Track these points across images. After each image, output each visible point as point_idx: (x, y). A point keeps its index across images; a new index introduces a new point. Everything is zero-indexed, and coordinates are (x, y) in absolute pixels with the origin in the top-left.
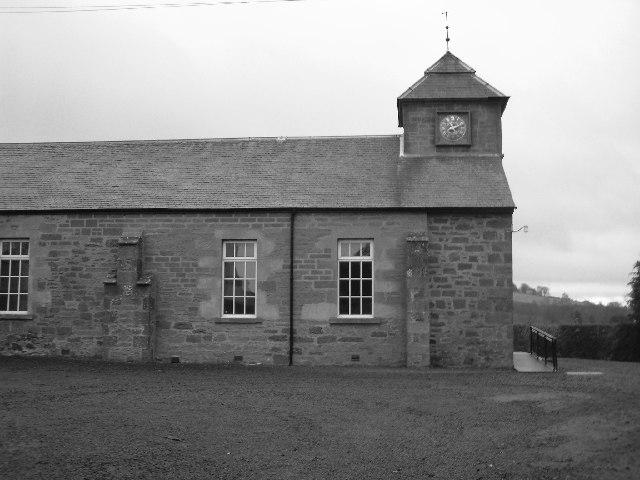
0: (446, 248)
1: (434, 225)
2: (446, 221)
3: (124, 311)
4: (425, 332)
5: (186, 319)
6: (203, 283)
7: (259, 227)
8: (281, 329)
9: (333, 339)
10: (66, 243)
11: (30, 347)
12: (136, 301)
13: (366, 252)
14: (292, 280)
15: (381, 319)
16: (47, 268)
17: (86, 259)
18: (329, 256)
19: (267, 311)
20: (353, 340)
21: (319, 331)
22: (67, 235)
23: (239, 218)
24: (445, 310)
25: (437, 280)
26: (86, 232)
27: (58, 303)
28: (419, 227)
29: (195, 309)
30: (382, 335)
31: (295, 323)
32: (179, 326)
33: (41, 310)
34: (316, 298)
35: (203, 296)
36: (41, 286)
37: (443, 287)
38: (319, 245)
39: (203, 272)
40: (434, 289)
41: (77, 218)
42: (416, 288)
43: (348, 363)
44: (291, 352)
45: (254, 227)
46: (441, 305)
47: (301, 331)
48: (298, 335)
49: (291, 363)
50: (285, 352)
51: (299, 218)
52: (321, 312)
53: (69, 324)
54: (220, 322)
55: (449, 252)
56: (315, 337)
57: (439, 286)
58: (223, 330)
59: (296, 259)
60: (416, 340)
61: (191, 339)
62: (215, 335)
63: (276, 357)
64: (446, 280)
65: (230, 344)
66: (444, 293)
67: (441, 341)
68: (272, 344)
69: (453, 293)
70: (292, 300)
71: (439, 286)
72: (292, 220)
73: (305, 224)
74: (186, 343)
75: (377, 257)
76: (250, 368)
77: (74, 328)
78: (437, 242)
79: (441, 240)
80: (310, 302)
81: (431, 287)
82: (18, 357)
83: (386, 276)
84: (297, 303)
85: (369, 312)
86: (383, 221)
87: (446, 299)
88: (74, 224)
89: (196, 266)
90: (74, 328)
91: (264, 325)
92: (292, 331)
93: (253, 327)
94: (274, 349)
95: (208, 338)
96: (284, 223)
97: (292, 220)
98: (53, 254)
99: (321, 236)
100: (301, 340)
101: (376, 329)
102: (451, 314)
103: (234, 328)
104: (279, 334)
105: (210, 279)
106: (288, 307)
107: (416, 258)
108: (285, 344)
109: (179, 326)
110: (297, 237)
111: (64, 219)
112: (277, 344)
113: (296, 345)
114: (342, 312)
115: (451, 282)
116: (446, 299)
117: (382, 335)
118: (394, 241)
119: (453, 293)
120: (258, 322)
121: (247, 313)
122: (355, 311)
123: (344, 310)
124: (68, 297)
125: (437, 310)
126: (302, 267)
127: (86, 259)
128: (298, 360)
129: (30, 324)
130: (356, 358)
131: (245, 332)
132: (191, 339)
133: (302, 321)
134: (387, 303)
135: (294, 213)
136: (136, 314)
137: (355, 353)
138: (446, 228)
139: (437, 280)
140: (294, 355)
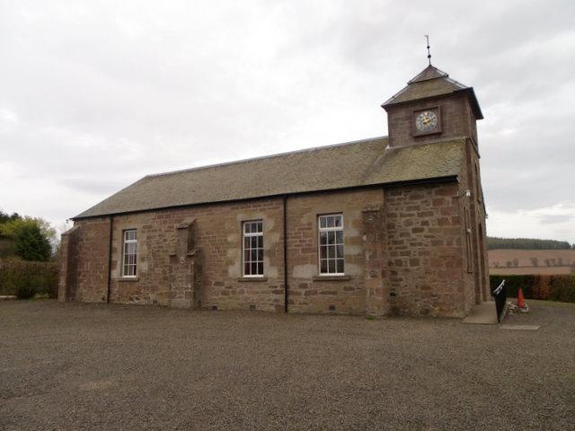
0: (402, 215)
1: (390, 197)
2: (400, 194)
3: (180, 275)
4: (380, 286)
5: (221, 280)
6: (231, 253)
7: (264, 210)
8: (279, 285)
9: (315, 293)
10: (156, 230)
11: (137, 299)
12: (187, 267)
13: (337, 224)
14: (285, 248)
15: (349, 276)
16: (145, 247)
17: (165, 240)
18: (310, 229)
19: (272, 272)
20: (330, 293)
21: (305, 286)
22: (156, 225)
23: (275, 203)
24: (403, 267)
25: (395, 242)
26: (165, 222)
27: (151, 269)
28: (377, 200)
29: (226, 272)
30: (352, 289)
31: (289, 280)
32: (217, 284)
33: (142, 274)
34: (303, 261)
35: (231, 263)
36: (143, 260)
37: (399, 248)
38: (304, 220)
39: (230, 245)
40: (393, 250)
41: (160, 214)
42: (370, 250)
43: (325, 312)
44: (286, 303)
45: (261, 210)
46: (399, 263)
47: (293, 287)
48: (292, 289)
49: (286, 311)
50: (282, 303)
51: (115, 219)
52: (305, 272)
53: (156, 283)
54: (241, 281)
55: (404, 219)
56: (303, 291)
57: (396, 248)
58: (243, 286)
59: (288, 232)
60: (372, 294)
61: (224, 293)
62: (238, 290)
63: (276, 306)
64: (401, 242)
65: (249, 295)
66: (402, 254)
67: (400, 293)
68: (274, 296)
69: (408, 254)
70: (286, 263)
71: (396, 248)
72: (112, 221)
73: (294, 205)
74: (221, 296)
75: (346, 226)
76: (259, 312)
77: (160, 286)
78: (393, 211)
79: (397, 209)
80: (298, 264)
81: (390, 249)
82: (131, 305)
83: (354, 241)
84: (289, 266)
85: (342, 271)
86: (349, 197)
87: (402, 258)
88: (159, 217)
89: (226, 240)
90: (160, 286)
91: (268, 282)
92: (286, 286)
93: (262, 283)
94: (276, 300)
95: (234, 292)
96: (278, 207)
97: (112, 221)
98: (148, 238)
99: (306, 212)
100: (294, 293)
101: (347, 285)
102: (407, 270)
103: (250, 285)
104: (278, 289)
105: (235, 250)
106: (283, 268)
107: (376, 227)
108: (282, 297)
109: (217, 284)
110: (289, 215)
111: (153, 215)
112: (277, 296)
113: (290, 297)
114: (322, 272)
115: (407, 244)
116: (402, 258)
117: (352, 289)
118: (358, 214)
119: (408, 254)
120: (265, 280)
121: (259, 273)
122: (332, 271)
123: (324, 271)
124: (156, 266)
125: (395, 268)
126: (293, 238)
127: (165, 240)
128: (292, 309)
129: (137, 284)
130: (332, 308)
131: (257, 288)
132: (224, 293)
133: (295, 279)
134: (355, 263)
135: (285, 198)
136: (187, 276)
137: (332, 304)
138: (401, 199)
139: (395, 242)
140: (289, 305)
